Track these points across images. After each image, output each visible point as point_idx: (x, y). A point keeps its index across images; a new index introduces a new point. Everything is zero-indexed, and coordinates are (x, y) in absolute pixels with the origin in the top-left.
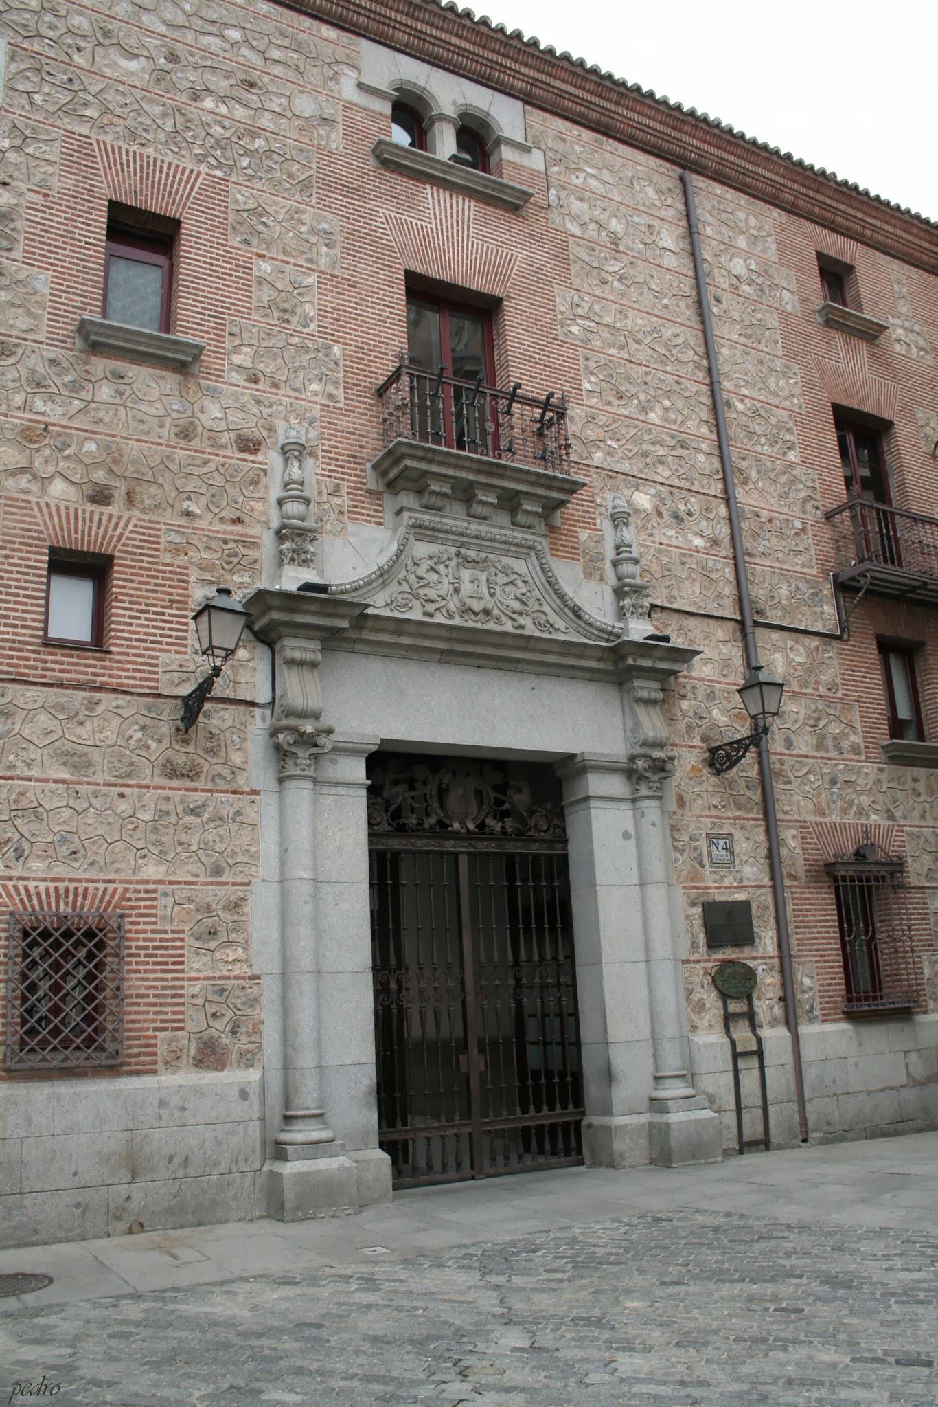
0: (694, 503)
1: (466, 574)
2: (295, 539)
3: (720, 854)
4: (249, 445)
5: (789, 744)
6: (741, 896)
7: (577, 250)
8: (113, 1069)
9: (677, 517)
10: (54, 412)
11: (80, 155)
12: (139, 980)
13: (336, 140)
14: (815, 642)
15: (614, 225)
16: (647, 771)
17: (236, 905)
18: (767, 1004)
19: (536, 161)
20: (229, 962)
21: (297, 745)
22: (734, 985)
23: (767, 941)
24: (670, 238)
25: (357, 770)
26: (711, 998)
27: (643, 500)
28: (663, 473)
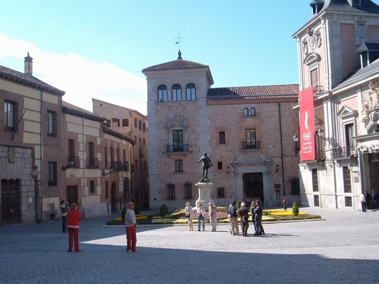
0: (277, 145)
1: (251, 158)
2: (235, 159)
3: (277, 180)
4: (232, 151)
5: (287, 168)
6: (279, 184)
7: (264, 119)
8: (224, 197)
9: (275, 147)
10: (216, 151)
11: (217, 128)
12: (226, 191)
13: (238, 117)
14: (292, 157)
15: (270, 115)
16: (269, 173)
17: (232, 187)
18: (282, 193)
19: (260, 111)
20: (232, 190)
21: (236, 174)
22: (278, 191)
23: (282, 187)
24: (277, 113)
25: (241, 176)
26: (275, 193)
27: (270, 146)
28: (273, 143)
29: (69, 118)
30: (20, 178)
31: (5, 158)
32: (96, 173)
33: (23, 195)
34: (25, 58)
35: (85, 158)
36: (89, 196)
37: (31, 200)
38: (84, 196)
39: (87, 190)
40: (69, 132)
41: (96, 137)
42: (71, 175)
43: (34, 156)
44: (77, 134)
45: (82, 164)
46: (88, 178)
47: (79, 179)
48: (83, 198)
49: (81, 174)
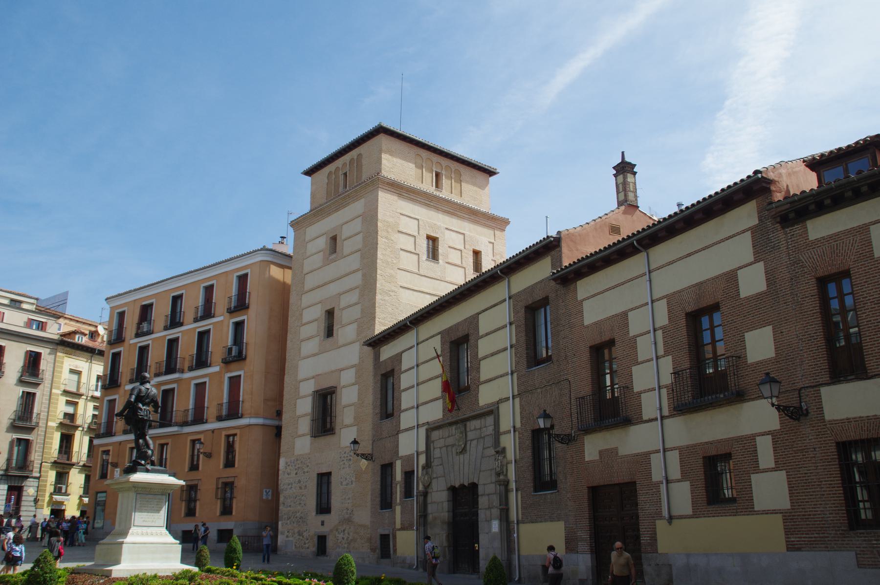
29: (585, 287)
30: (476, 481)
31: (453, 446)
32: (758, 417)
33: (482, 515)
34: (614, 168)
35: (667, 379)
36: (695, 515)
37: (495, 526)
38: (671, 518)
39: (682, 496)
40: (587, 327)
41: (731, 278)
42: (600, 452)
43: (499, 428)
44: (624, 315)
45: (650, 405)
46: (686, 452)
47: (644, 459)
48: (661, 525)
49: (657, 440)
